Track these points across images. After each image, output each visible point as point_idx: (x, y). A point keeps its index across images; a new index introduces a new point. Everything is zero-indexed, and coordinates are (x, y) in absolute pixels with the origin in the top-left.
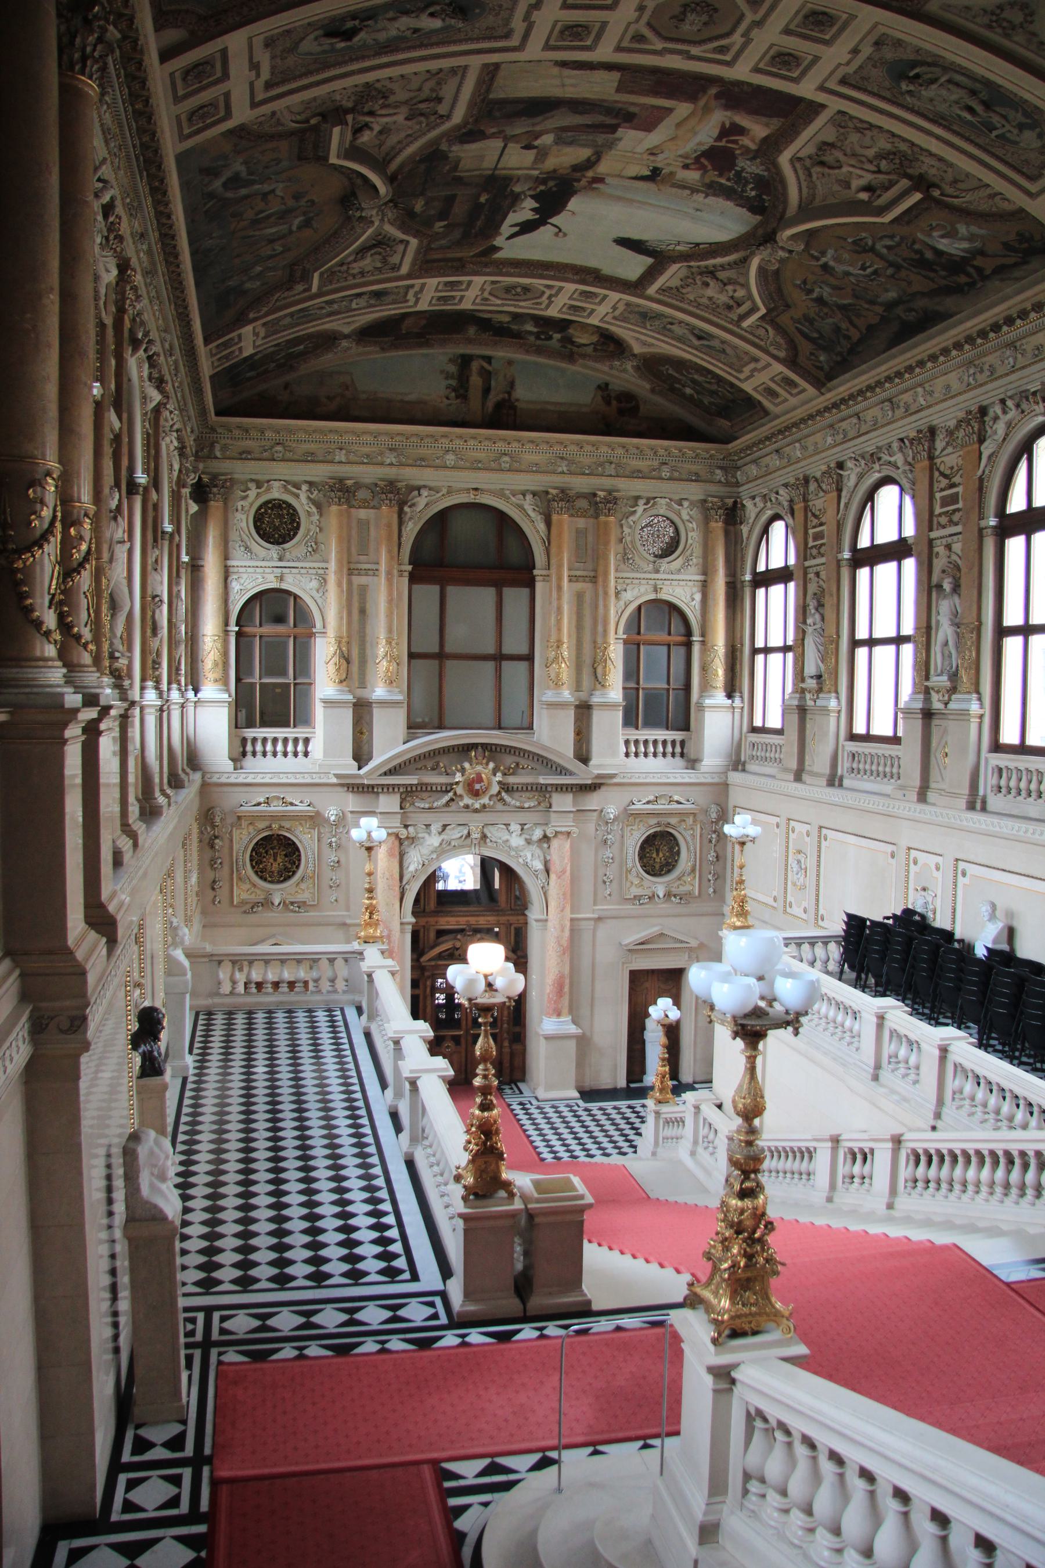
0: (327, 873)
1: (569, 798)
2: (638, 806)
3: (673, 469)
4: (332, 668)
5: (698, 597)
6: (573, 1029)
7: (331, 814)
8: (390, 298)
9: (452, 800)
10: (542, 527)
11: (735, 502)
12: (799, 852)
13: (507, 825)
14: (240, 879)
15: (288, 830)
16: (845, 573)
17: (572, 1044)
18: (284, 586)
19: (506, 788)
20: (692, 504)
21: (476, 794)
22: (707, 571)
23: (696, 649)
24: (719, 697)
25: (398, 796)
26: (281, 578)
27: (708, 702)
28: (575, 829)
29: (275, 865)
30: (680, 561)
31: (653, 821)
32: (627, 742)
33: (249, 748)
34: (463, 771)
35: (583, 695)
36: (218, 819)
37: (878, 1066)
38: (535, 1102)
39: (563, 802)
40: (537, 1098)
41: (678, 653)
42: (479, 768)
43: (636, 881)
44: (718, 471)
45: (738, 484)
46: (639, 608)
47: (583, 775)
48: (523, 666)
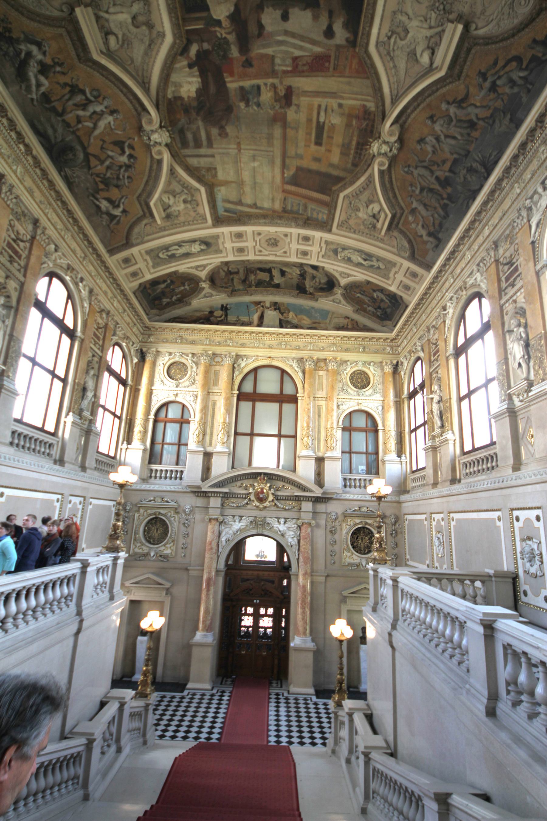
0: (182, 541)
1: (310, 504)
2: (349, 512)
3: (364, 348)
4: (195, 437)
5: (380, 408)
6: (311, 645)
7: (187, 508)
8: (213, 248)
9: (247, 504)
10: (300, 374)
11: (398, 362)
12: (439, 532)
13: (278, 518)
14: (135, 540)
15: (165, 515)
16: (452, 362)
17: (310, 656)
18: (178, 399)
19: (277, 498)
20: (375, 363)
21: (261, 500)
22: (385, 395)
23: (381, 433)
24: (392, 455)
25: (220, 499)
26: (177, 395)
27: (387, 458)
28: (313, 522)
29: (156, 534)
30: (371, 391)
31: (358, 521)
32: (345, 479)
33: (153, 475)
34: (253, 486)
35: (320, 454)
36: (128, 508)
37: (493, 697)
38: (286, 694)
39: (307, 506)
40: (289, 693)
41: (371, 436)
42: (262, 486)
43: (349, 554)
44: (388, 348)
45: (399, 354)
46: (350, 413)
47: (318, 492)
48: (293, 439)
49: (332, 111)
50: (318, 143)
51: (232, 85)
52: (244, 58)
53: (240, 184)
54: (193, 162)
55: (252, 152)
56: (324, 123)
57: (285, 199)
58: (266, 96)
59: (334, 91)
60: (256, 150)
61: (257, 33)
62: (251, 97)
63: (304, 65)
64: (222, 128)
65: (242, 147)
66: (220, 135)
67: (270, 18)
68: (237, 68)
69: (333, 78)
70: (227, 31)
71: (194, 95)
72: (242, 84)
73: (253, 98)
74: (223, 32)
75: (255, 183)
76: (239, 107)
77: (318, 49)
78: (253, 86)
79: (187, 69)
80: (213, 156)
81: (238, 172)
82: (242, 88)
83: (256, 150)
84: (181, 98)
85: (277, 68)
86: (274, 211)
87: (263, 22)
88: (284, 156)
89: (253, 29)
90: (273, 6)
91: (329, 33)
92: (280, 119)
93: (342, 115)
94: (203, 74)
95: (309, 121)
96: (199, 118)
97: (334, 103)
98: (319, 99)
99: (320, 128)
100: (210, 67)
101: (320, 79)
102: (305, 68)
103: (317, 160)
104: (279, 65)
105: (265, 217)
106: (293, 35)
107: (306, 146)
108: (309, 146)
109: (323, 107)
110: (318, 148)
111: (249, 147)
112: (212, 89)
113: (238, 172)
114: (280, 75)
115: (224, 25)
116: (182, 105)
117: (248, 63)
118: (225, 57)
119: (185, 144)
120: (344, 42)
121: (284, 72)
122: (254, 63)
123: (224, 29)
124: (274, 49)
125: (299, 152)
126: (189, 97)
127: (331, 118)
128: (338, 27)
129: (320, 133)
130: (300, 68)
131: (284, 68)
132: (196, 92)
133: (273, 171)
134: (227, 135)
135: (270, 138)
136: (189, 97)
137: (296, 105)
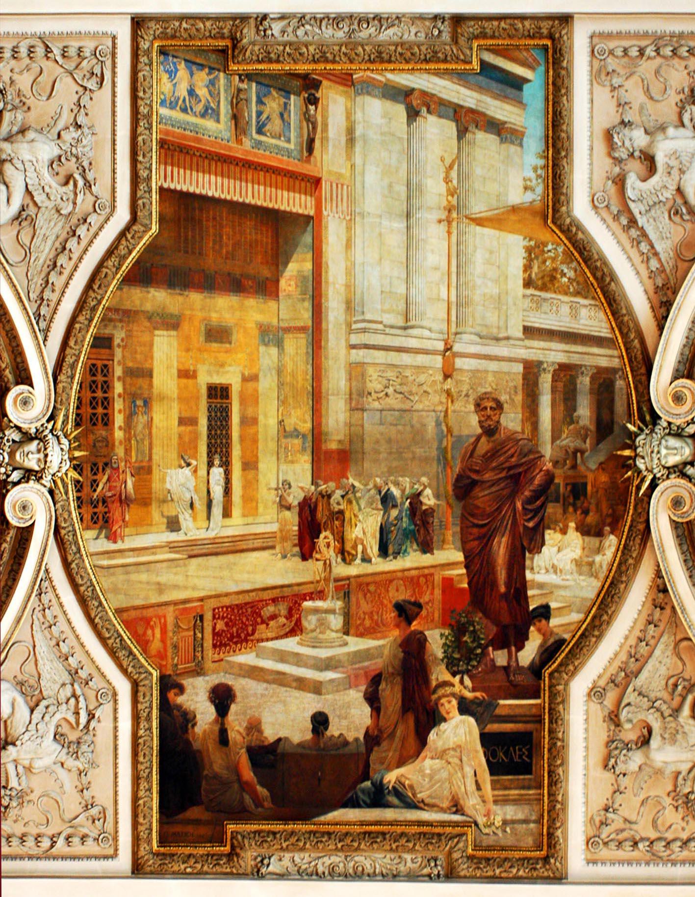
49: (192, 505)
50: (219, 394)
51: (449, 556)
52: (415, 626)
53: (455, 213)
54: (591, 319)
55: (413, 343)
56: (210, 464)
57: (311, 142)
58: (365, 527)
59: (194, 561)
60: (400, 350)
61: (383, 686)
62: (405, 522)
63: (273, 617)
64: (490, 430)
65: (438, 361)
66: (499, 406)
67: (352, 717)
68: (433, 600)
69: (202, 594)
70: (448, 690)
71: (551, 536)
72: (426, 560)
73: (399, 518)
74: (458, 688)
75: (408, 216)
76: (437, 496)
77: (246, 658)
78: (396, 554)
79: (553, 605)
80: (529, 332)
81: (458, 260)
82: (426, 547)
83: (400, 350)
84: (585, 530)
85: (339, 604)
86: (346, 80)
87: (367, 710)
88: (316, 334)
89: (392, 695)
90: (346, 743)
91: (222, 698)
92: (332, 460)
93: (167, 499)
94: (518, 588)
95: (250, 465)
96: (549, 466)
97: (193, 529)
98: (229, 532)
99: (219, 447)
100: (498, 607)
101: (233, 588)
102: (271, 609)
103: (218, 334)
104: (332, 611)
105: (381, 57)
106: (301, 684)
107: (254, 378)
108: (245, 379)
109: (217, 511)
110: (217, 380)
111: (420, 359)
112: (501, 548)
113: (458, 260)
114: (332, 585)
115: (454, 702)
116: (586, 512)
117: (406, 612)
118: (459, 630)
119: (604, 383)
120: (187, 682)
121: (320, 595)
122: (391, 615)
123: (453, 695)
124: (345, 650)
125: (274, 351)
126: (564, 532)
127: (192, 483)
128: (205, 713)
129: (218, 424)
130: (283, 609)
131: (319, 604)
132: (543, 544)
133: (350, 271)
134: (479, 406)
135: (357, 399)
136: (564, 532)
137: (289, 508)
